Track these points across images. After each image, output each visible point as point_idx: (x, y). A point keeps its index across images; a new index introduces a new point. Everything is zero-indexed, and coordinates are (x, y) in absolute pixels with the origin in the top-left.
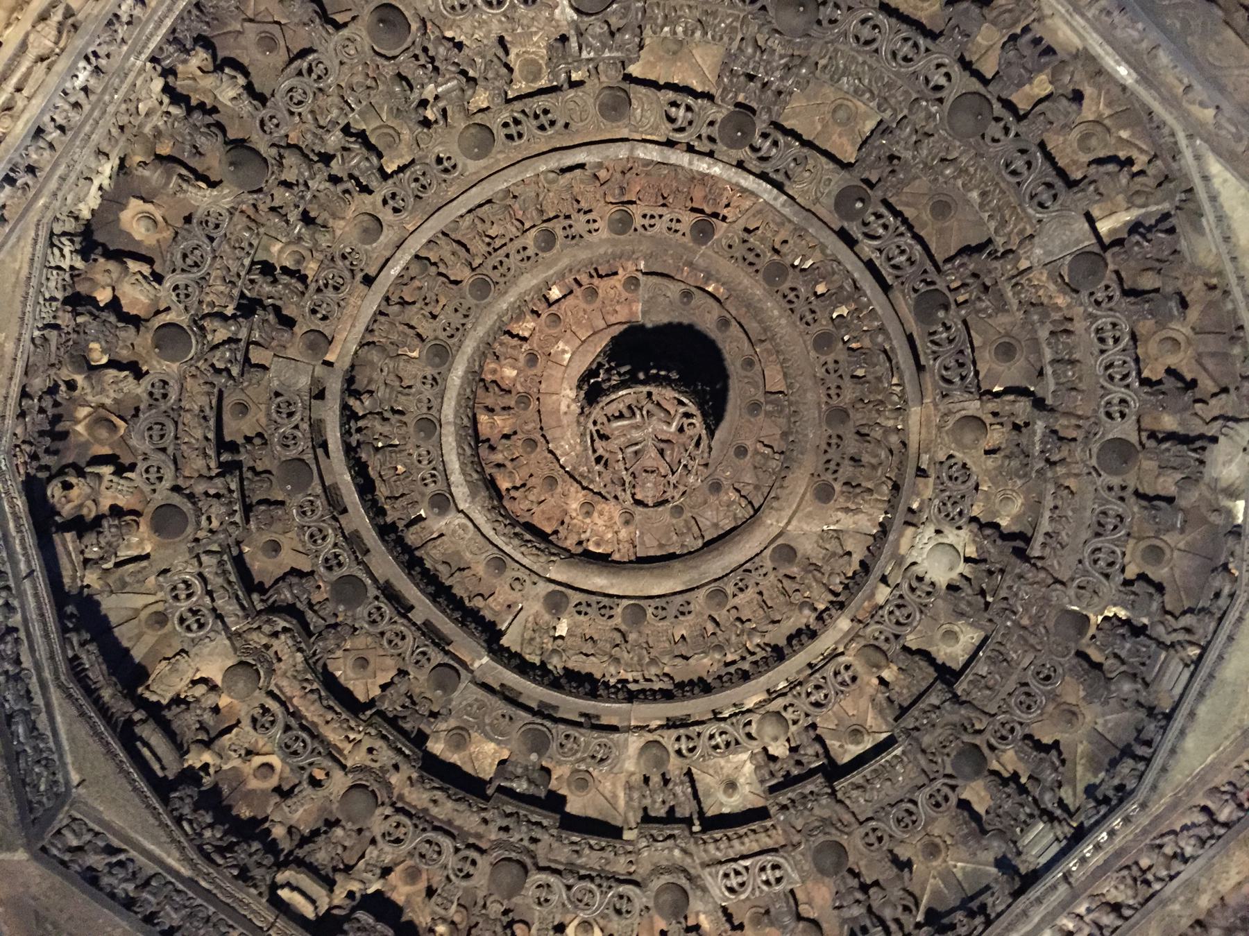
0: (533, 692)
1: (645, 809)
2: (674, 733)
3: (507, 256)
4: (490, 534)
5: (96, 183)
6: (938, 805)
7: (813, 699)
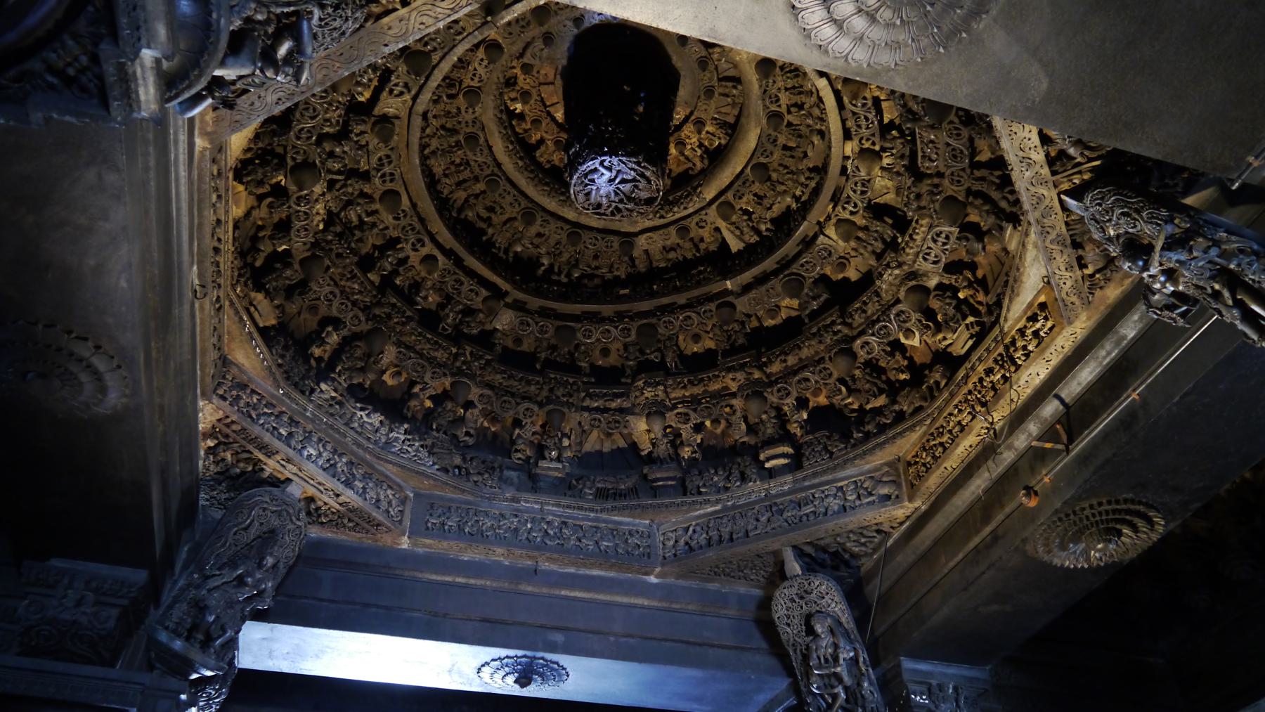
0: (769, 264)
1: (874, 252)
2: (839, 208)
4: (662, 221)
5: (366, 419)
6: (959, 135)
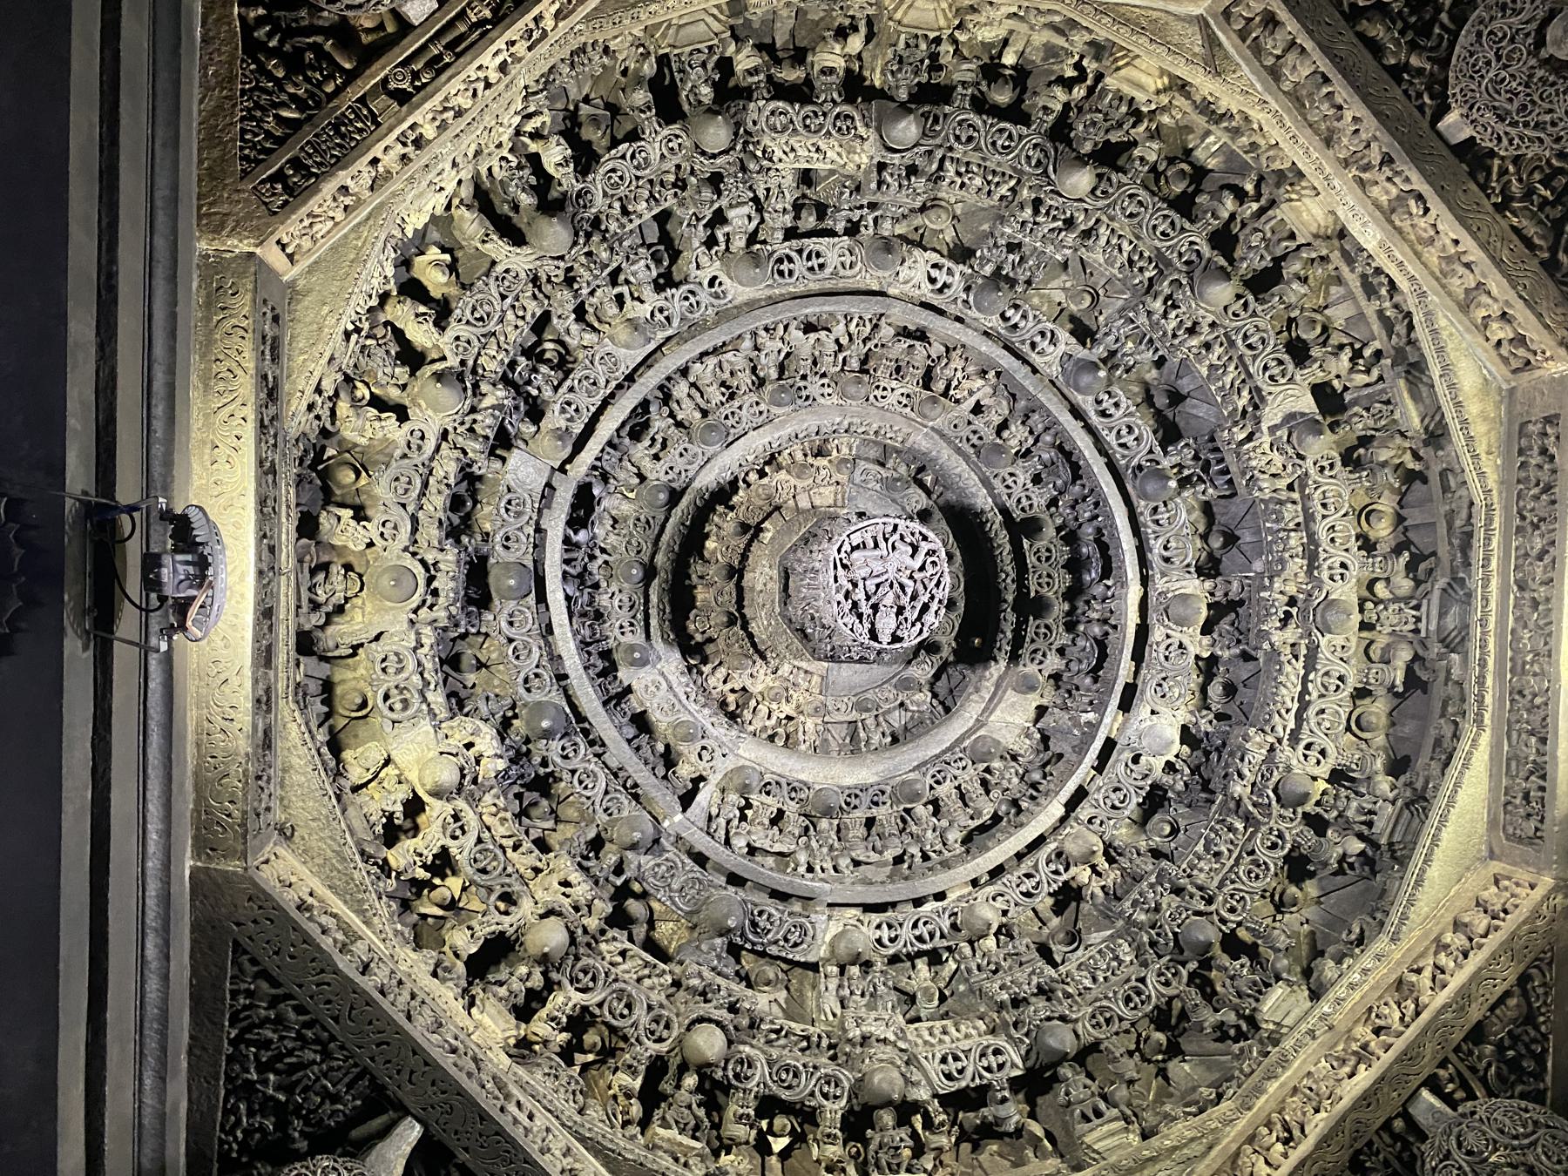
3: (740, 408)
7: (1023, 888)
